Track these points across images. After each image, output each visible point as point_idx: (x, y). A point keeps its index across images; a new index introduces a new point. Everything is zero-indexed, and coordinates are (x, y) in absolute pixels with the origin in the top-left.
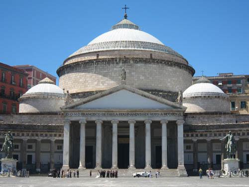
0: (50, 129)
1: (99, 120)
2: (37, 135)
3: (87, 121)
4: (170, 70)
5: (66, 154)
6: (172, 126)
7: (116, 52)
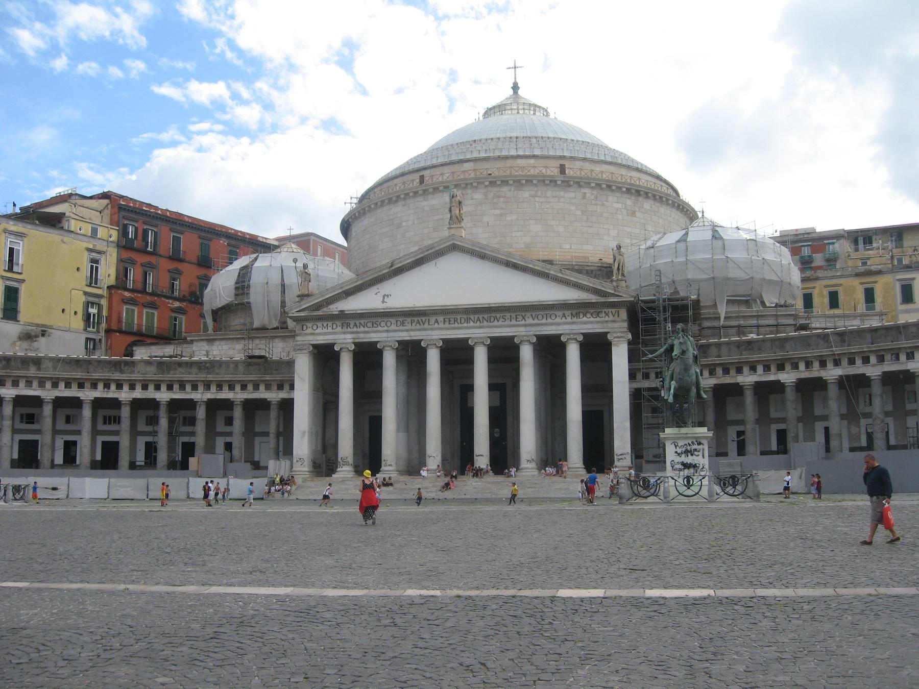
3: (356, 344)
4: (620, 206)
5: (303, 436)
7: (467, 166)
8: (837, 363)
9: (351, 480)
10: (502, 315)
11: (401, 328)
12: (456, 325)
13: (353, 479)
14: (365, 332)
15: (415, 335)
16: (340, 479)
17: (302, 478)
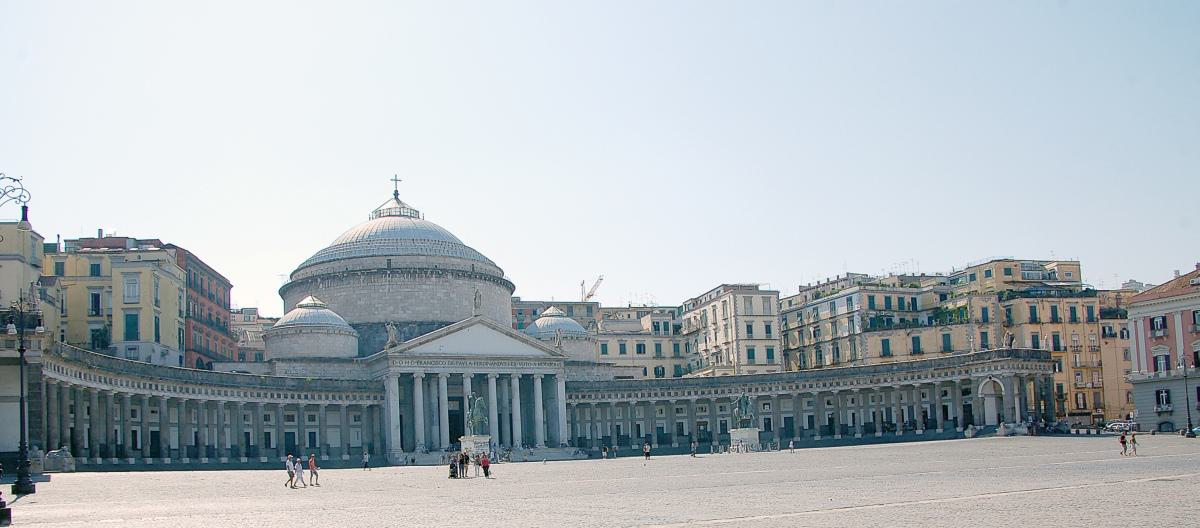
0: (359, 387)
1: (444, 371)
2: (340, 398)
6: (548, 381)
7: (421, 258)
8: (656, 395)
15: (459, 371)
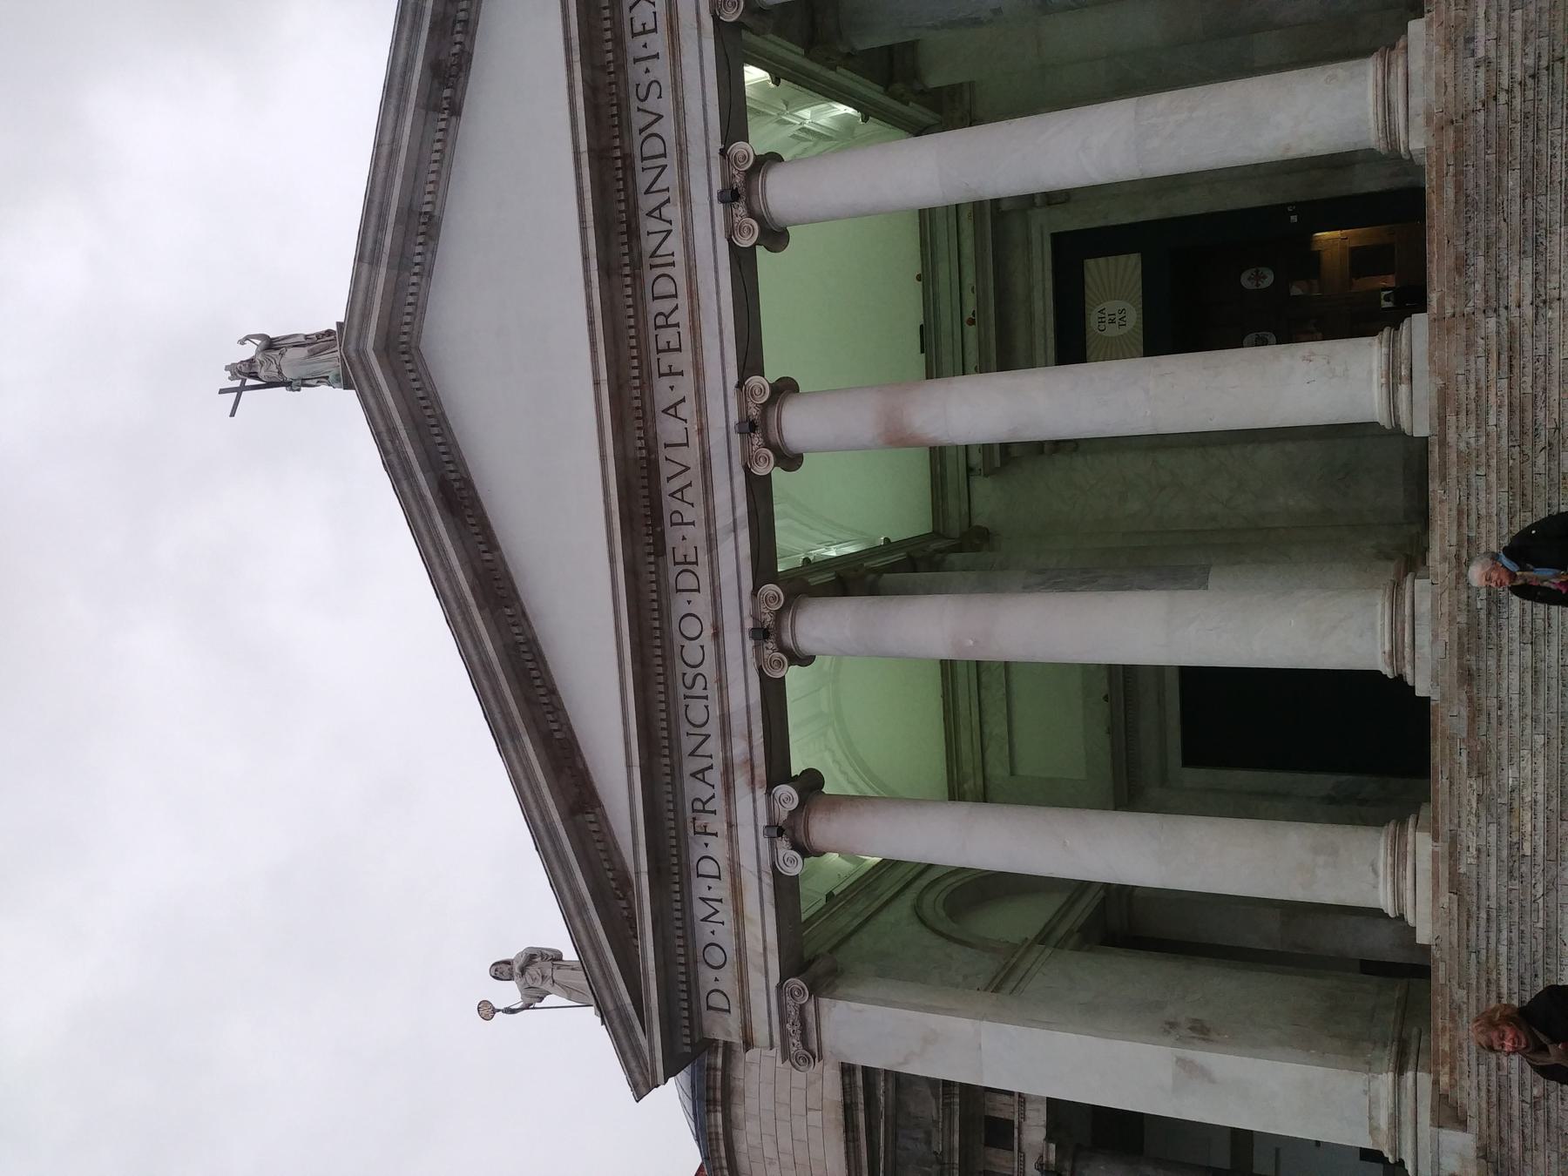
9: (1454, 840)
10: (634, 103)
11: (703, 571)
12: (682, 317)
13: (1445, 828)
14: (726, 733)
16: (1445, 899)
17: (1438, 1124)
